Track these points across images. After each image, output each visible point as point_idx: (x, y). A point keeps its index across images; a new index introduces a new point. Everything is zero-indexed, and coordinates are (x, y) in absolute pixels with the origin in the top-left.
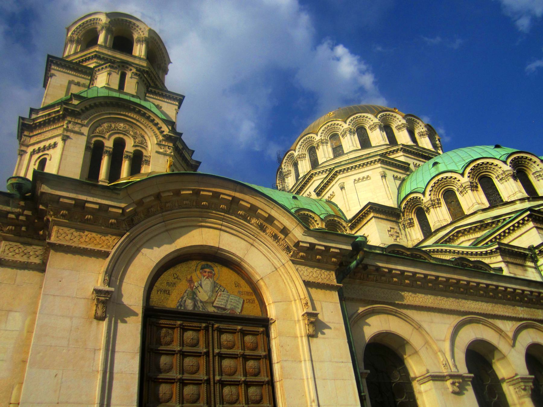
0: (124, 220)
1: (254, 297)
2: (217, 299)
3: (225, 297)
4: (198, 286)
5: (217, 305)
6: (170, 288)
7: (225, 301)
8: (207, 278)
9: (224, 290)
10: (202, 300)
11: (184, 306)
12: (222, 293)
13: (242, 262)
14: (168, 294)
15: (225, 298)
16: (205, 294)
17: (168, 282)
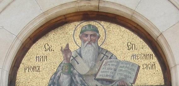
1: (155, 60)
2: (101, 70)
3: (112, 65)
4: (77, 56)
5: (101, 77)
7: (112, 71)
8: (89, 43)
9: (112, 56)
10: (81, 73)
11: (58, 83)
12: (109, 60)
13: (134, 15)
14: (38, 71)
15: (113, 67)
16: (85, 65)
17: (38, 56)
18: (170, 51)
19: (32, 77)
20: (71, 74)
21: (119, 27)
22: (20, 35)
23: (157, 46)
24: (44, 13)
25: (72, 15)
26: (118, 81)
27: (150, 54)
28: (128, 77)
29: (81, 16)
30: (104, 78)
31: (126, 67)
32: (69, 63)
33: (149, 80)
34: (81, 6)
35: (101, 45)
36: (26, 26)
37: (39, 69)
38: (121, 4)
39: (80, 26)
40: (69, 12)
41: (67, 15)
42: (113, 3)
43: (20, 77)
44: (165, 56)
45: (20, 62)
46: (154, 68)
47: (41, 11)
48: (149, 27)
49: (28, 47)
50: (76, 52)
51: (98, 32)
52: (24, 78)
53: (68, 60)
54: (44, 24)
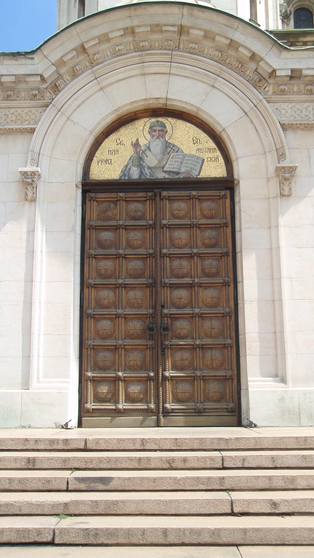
0: (46, 88)
1: (218, 153)
2: (168, 163)
3: (179, 158)
4: (146, 150)
5: (168, 170)
6: (112, 157)
8: (157, 138)
9: (178, 150)
11: (129, 175)
12: (176, 153)
13: (198, 112)
15: (179, 160)
16: (153, 158)
17: (110, 149)
18: (232, 145)
19: (105, 170)
20: (141, 167)
21: (185, 123)
22: (93, 131)
23: (220, 141)
24: (116, 110)
25: (142, 112)
26: (184, 173)
27: (214, 148)
28: (194, 169)
29: (150, 113)
30: (171, 170)
31: (192, 160)
32: (139, 156)
33: (213, 172)
34: (150, 104)
35: (168, 140)
36: (99, 121)
37: (111, 161)
38: (187, 101)
39: (149, 122)
40: (139, 109)
41: (137, 111)
42: (180, 101)
43: (93, 169)
44: (227, 150)
45: (94, 156)
46: (217, 160)
47: (113, 108)
48: (213, 123)
49: (101, 141)
50: (146, 146)
51: (166, 128)
52: (97, 171)
53: (138, 153)
54: (116, 120)
